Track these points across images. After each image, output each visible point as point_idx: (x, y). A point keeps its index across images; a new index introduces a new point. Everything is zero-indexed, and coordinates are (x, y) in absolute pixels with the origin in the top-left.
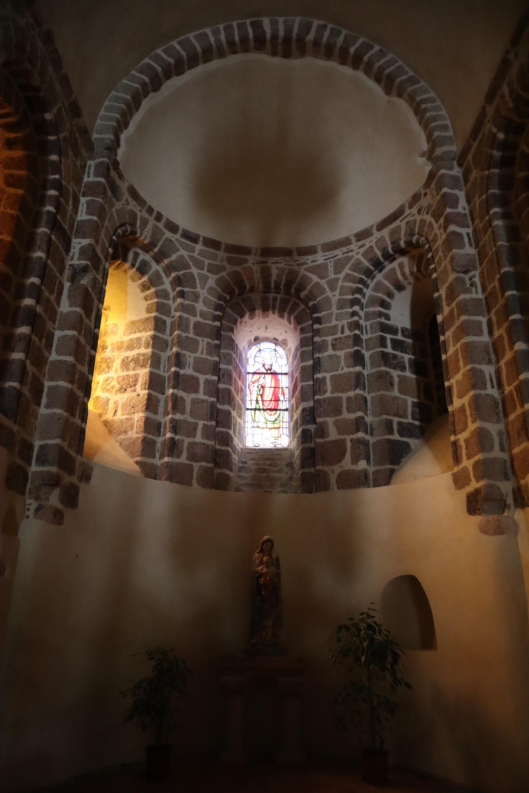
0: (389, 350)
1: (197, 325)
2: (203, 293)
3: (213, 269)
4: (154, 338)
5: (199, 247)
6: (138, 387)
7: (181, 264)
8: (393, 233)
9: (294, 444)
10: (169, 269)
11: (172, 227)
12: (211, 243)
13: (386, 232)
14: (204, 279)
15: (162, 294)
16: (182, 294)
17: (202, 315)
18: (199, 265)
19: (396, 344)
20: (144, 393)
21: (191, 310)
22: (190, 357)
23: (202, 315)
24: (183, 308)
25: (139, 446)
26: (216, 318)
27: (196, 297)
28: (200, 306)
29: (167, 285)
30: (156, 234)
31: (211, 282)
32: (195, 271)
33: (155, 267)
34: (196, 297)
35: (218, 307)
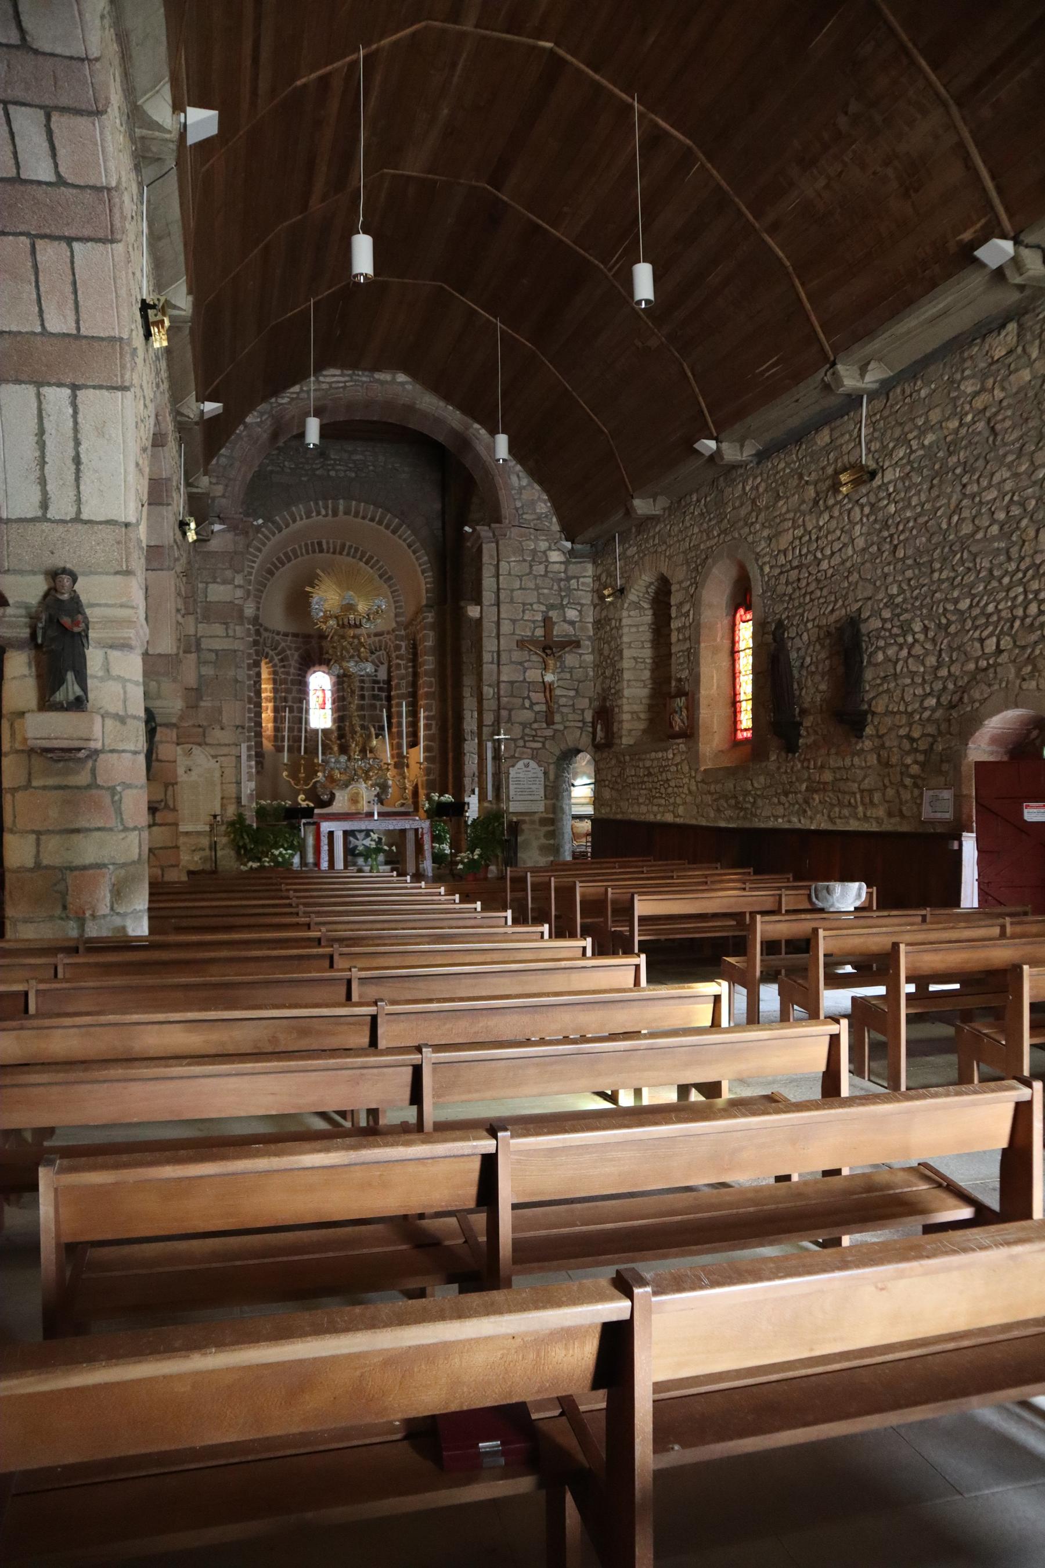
0: (376, 692)
1: (292, 680)
2: (293, 663)
3: (297, 649)
4: (274, 688)
5: (290, 638)
6: (269, 711)
7: (283, 651)
8: (380, 641)
9: (334, 728)
10: (278, 654)
11: (278, 633)
12: (295, 635)
13: (377, 639)
14: (292, 655)
15: (274, 666)
16: (284, 666)
17: (294, 675)
18: (290, 649)
19: (380, 689)
20: (272, 715)
21: (288, 673)
22: (290, 697)
23: (294, 675)
24: (283, 673)
25: (272, 738)
26: (299, 675)
27: (290, 666)
28: (292, 670)
29: (276, 659)
30: (273, 638)
31: (296, 657)
32: (288, 652)
33: (271, 653)
34: (290, 666)
35: (300, 669)
